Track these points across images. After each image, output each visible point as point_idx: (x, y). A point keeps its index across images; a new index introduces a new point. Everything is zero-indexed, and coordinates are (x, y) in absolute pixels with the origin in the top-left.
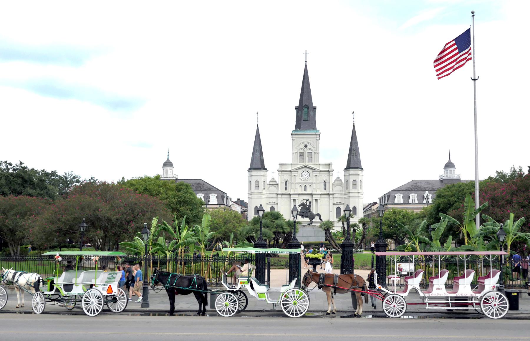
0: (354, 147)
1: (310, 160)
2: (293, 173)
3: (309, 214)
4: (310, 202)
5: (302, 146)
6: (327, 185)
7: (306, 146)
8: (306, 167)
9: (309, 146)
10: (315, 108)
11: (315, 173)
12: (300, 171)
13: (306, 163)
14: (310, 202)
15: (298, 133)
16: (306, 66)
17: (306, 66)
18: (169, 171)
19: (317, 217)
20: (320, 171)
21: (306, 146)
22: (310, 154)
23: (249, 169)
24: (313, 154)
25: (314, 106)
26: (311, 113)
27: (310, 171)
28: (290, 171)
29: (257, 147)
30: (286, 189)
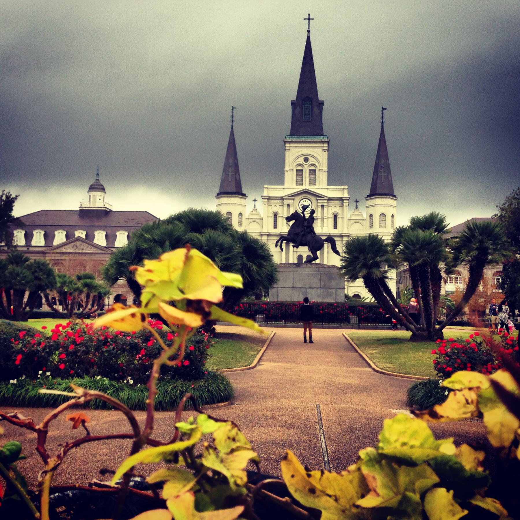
0: (382, 162)
1: (313, 182)
2: (286, 202)
3: (309, 237)
4: (313, 212)
5: (301, 160)
6: (339, 221)
7: (306, 160)
8: (306, 192)
9: (312, 161)
10: (322, 103)
11: (320, 202)
12: (298, 199)
13: (306, 186)
14: (313, 212)
15: (295, 139)
16: (308, 38)
17: (308, 38)
18: (98, 198)
19: (327, 247)
20: (329, 199)
21: (306, 160)
22: (313, 172)
23: (218, 194)
24: (317, 172)
25: (320, 99)
26: (316, 110)
27: (313, 199)
28: (282, 199)
29: (231, 161)
30: (275, 227)
